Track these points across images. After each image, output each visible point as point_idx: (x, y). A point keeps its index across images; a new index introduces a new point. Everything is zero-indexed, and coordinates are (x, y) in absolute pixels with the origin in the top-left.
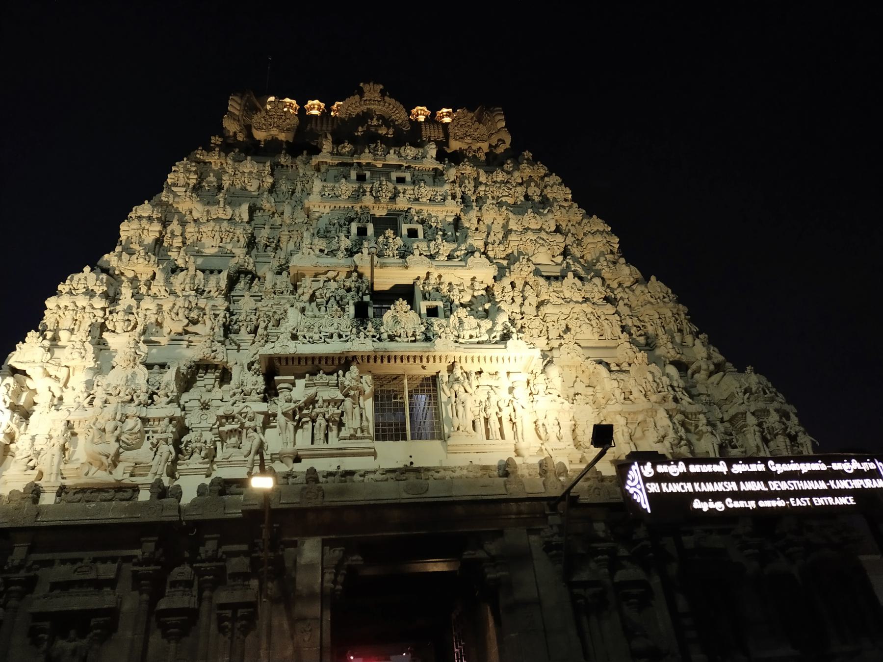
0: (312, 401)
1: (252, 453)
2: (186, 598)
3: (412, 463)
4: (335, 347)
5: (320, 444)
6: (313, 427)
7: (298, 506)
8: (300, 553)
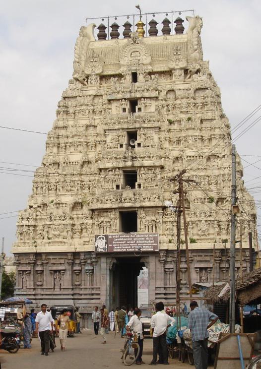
0: (102, 222)
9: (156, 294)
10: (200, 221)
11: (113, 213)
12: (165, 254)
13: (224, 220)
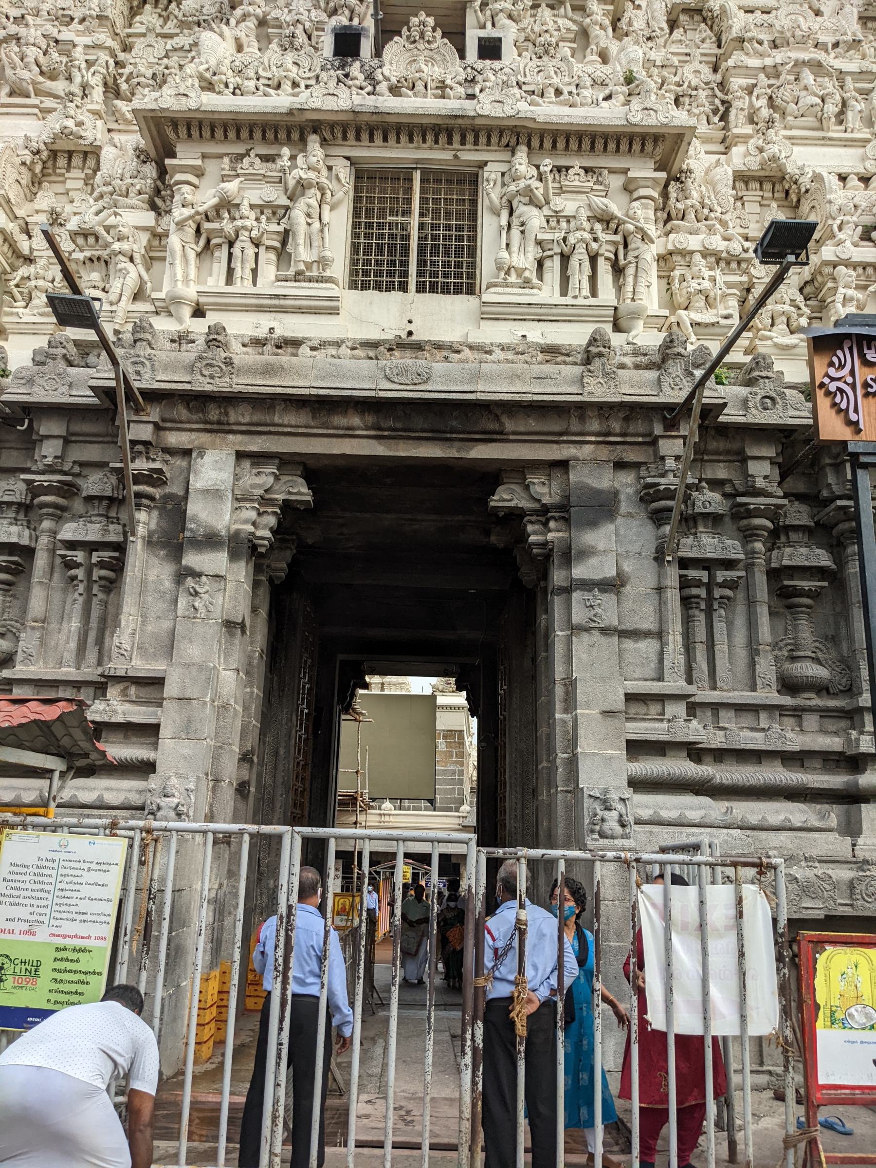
0: (226, 206)
1: (124, 298)
2: (14, 529)
3: (410, 333)
4: (280, 102)
6: (230, 255)
7: (188, 387)
9: (636, 748)
11: (315, 150)
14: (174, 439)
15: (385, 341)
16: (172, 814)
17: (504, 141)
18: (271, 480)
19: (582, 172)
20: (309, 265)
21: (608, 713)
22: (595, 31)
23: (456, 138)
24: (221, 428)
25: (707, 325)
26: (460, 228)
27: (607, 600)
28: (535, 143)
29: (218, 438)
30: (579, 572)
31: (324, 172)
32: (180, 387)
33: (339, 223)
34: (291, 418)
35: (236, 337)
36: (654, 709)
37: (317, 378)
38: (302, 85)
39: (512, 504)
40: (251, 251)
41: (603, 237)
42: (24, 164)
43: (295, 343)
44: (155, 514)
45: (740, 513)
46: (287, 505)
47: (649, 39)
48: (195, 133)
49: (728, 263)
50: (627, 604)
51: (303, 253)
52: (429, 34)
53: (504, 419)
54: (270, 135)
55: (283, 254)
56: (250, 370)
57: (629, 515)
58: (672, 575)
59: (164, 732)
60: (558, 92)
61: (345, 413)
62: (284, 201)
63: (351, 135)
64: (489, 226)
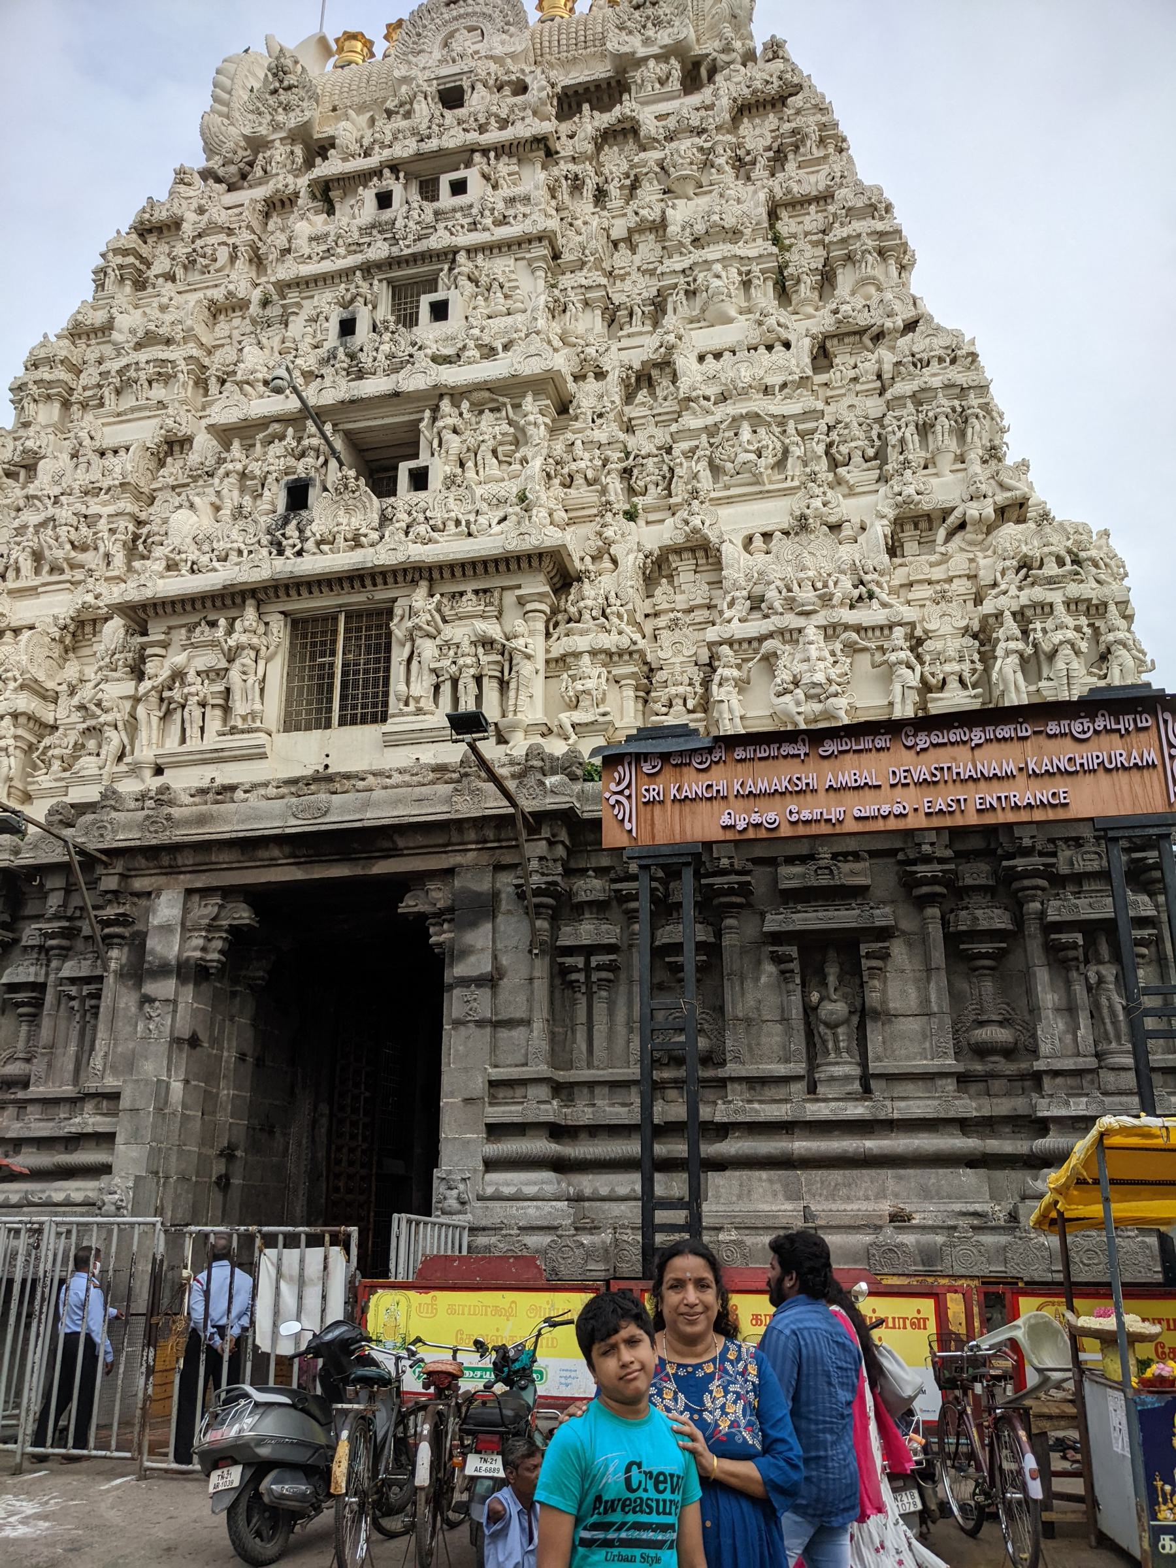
0: (178, 675)
2: (32, 969)
3: (327, 766)
5: (194, 743)
7: (138, 843)
8: (147, 911)
9: (495, 1131)
10: (792, 636)
11: (250, 613)
12: (560, 851)
13: (946, 629)
14: (138, 884)
15: (303, 778)
16: (113, 1208)
17: (409, 578)
18: (216, 909)
19: (474, 597)
20: (244, 718)
21: (468, 1101)
22: (531, 430)
23: (368, 582)
24: (172, 871)
25: (587, 724)
26: (377, 660)
27: (484, 994)
28: (436, 575)
29: (171, 879)
30: (460, 970)
31: (262, 629)
32: (132, 843)
33: (276, 671)
34: (224, 857)
35: (184, 790)
36: (519, 1092)
37: (238, 822)
38: (245, 553)
39: (416, 909)
40: (197, 712)
41: (484, 659)
42: (54, 640)
43: (232, 788)
44: (126, 949)
45: (622, 898)
46: (233, 930)
47: (600, 416)
48: (160, 611)
49: (620, 656)
50: (504, 994)
51: (239, 707)
52: (352, 484)
53: (396, 838)
54: (218, 603)
55: (226, 709)
56: (187, 822)
57: (509, 912)
58: (541, 968)
59: (119, 1139)
60: (458, 523)
61: (267, 847)
62: (223, 664)
63: (281, 593)
64: (399, 655)
